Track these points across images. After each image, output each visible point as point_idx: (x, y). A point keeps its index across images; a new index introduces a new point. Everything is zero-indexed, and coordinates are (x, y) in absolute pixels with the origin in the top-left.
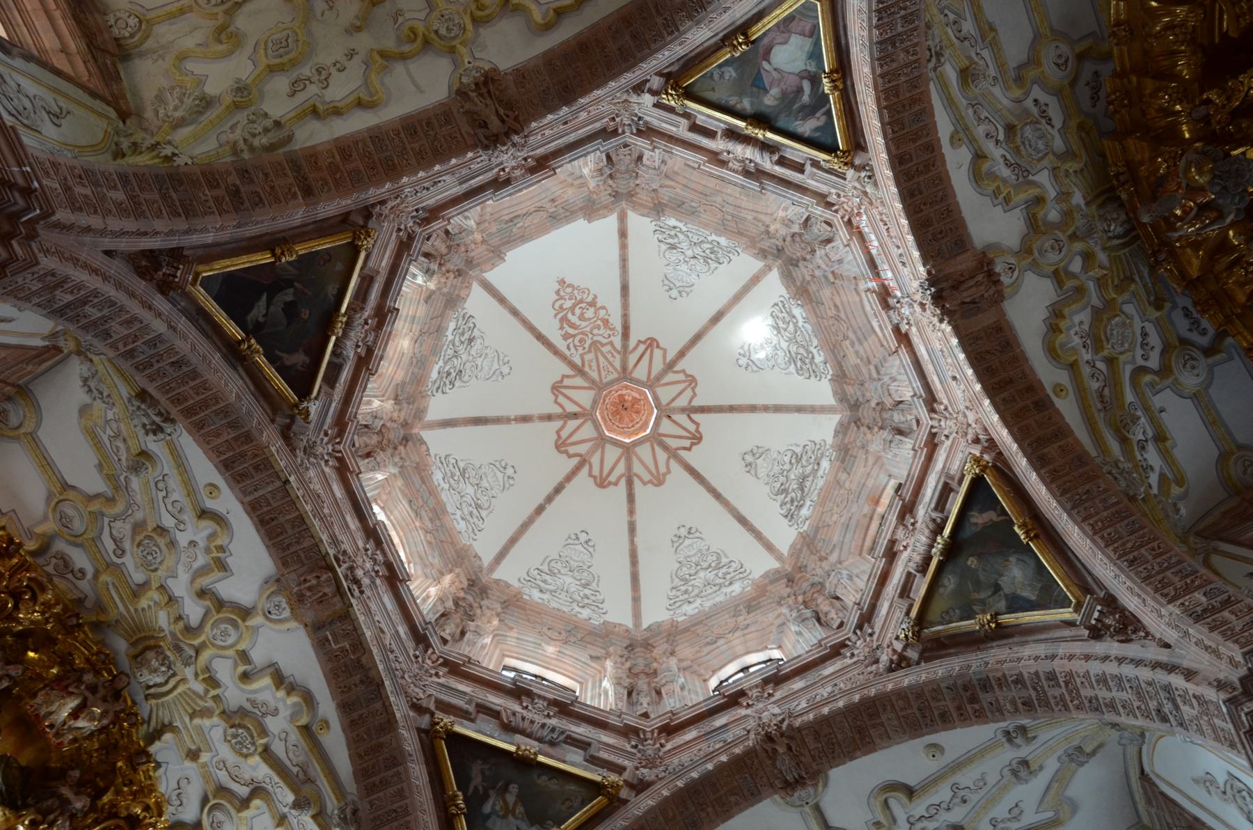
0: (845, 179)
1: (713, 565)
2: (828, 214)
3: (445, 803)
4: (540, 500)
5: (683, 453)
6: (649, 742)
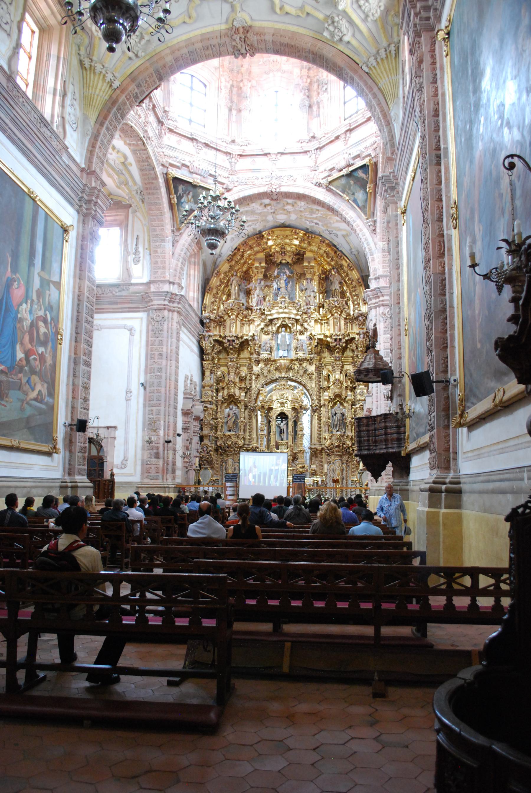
6: (233, 160)
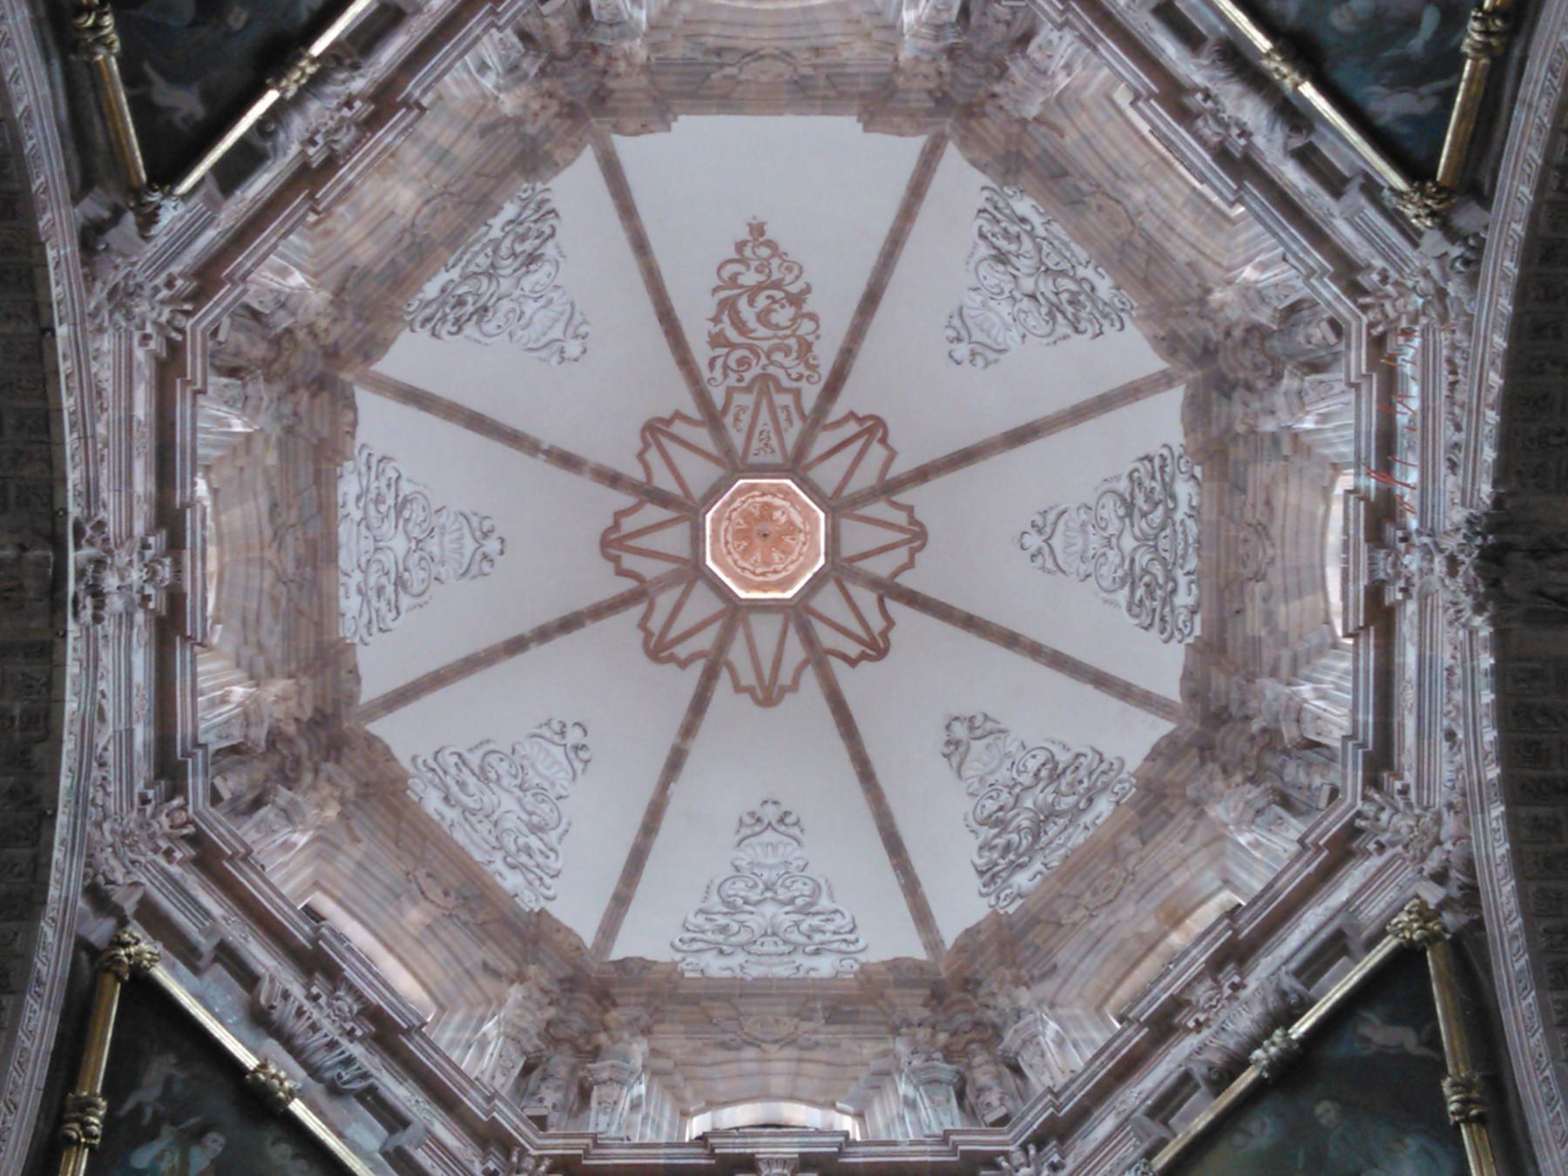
0: (1415, 245)
1: (799, 902)
2: (1345, 308)
3: (62, 1109)
4: (525, 627)
5: (837, 665)
